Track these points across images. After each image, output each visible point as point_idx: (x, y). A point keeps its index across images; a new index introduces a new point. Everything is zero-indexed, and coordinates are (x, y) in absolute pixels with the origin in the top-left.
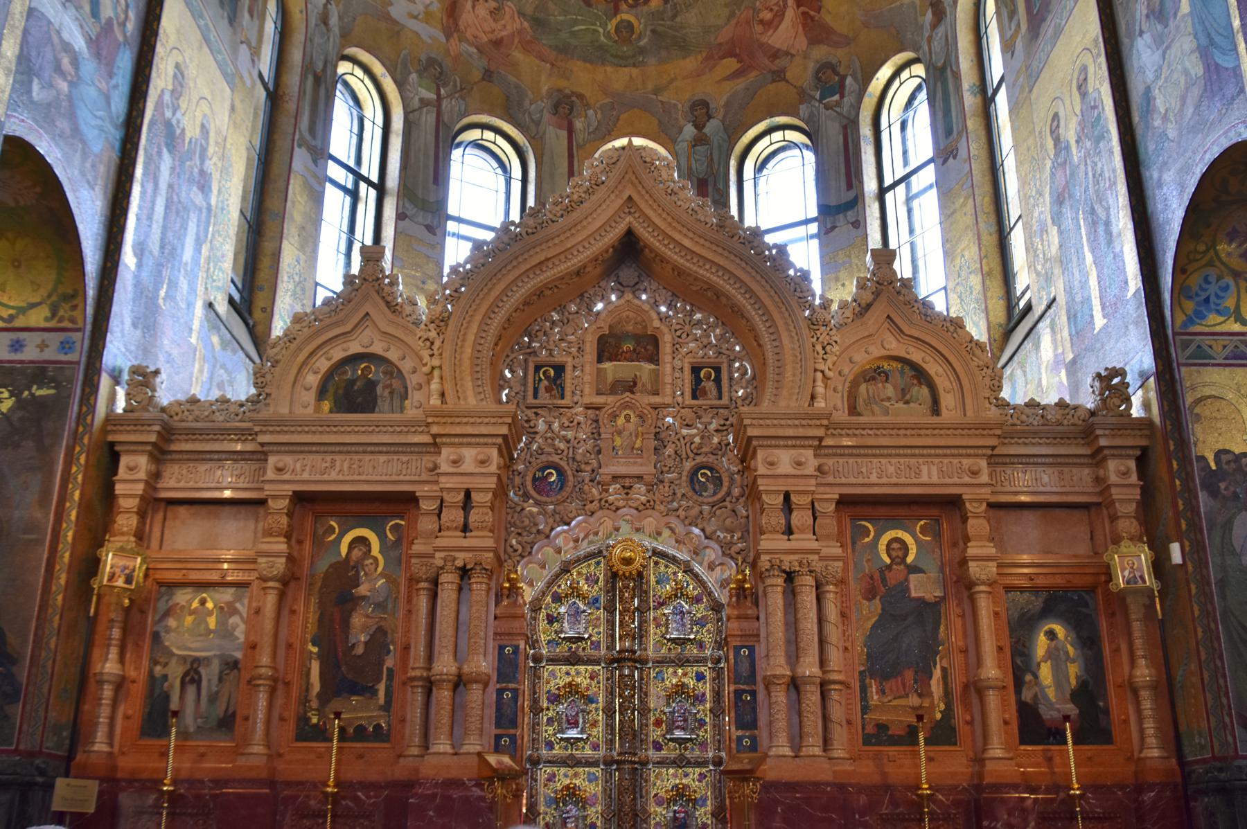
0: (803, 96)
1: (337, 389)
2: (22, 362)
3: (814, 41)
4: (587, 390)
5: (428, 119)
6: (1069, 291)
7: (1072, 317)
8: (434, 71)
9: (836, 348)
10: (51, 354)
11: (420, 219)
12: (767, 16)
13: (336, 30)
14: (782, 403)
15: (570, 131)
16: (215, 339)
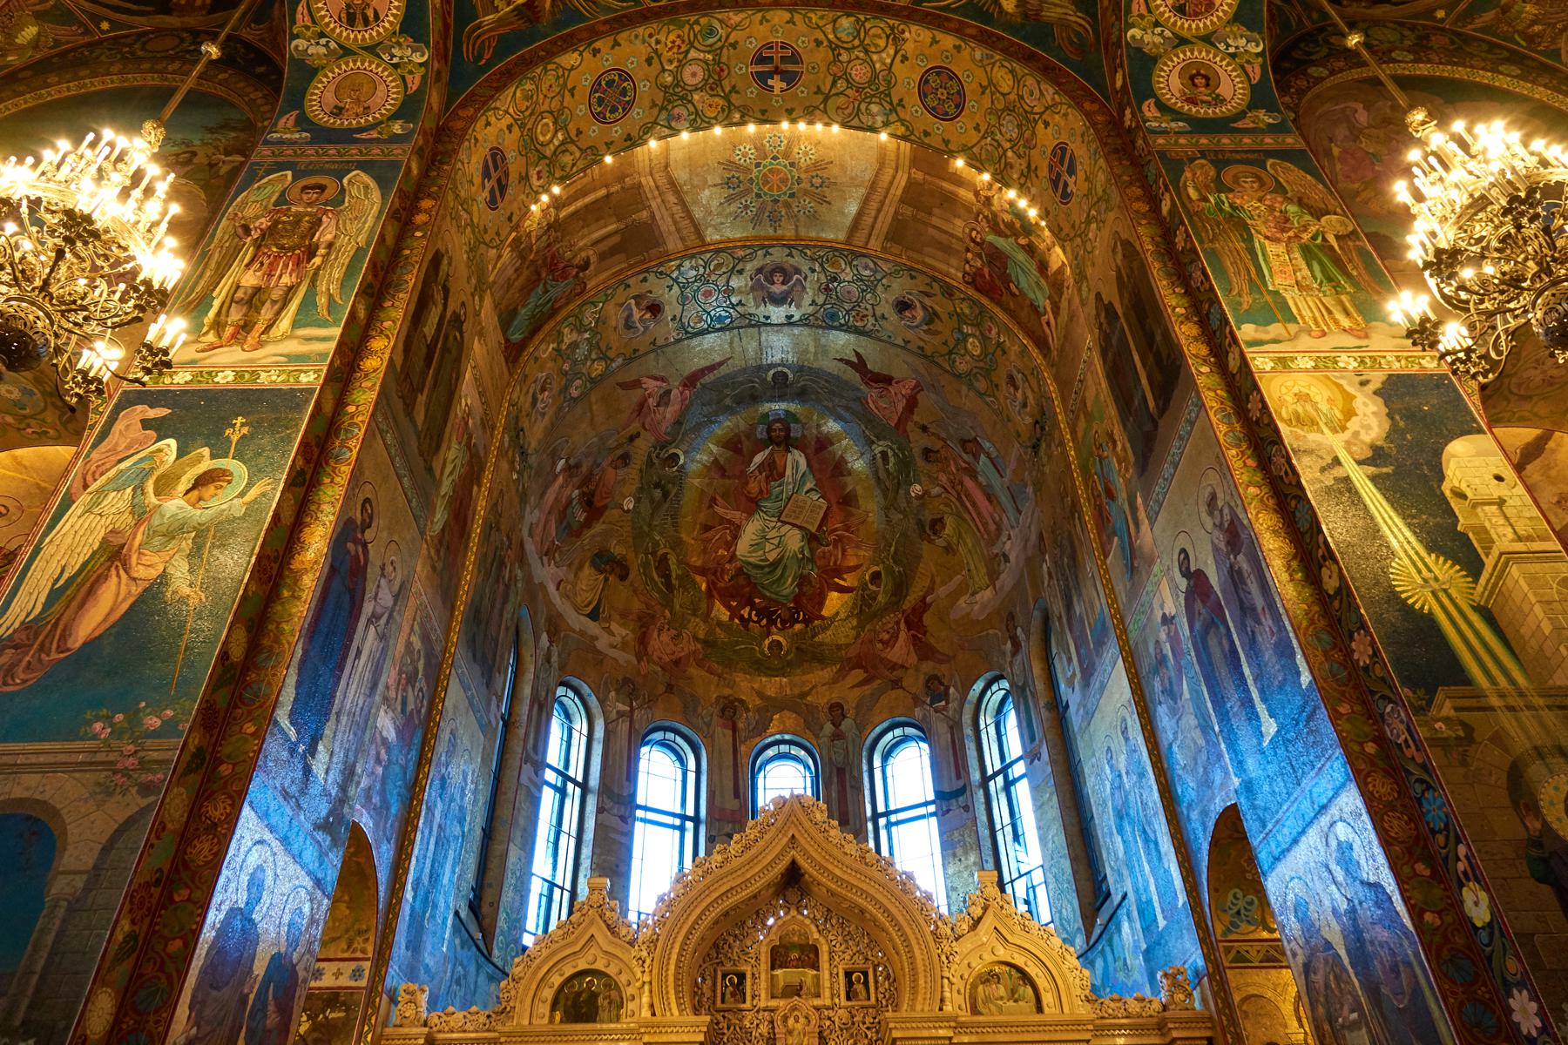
0: (917, 701)
1: (567, 999)
2: (319, 988)
3: (923, 658)
4: (763, 996)
5: (623, 727)
6: (1136, 891)
7: (1141, 913)
8: (629, 688)
9: (957, 959)
10: (344, 981)
11: (615, 811)
12: (886, 637)
13: (556, 665)
14: (919, 1007)
15: (734, 729)
16: (457, 941)
